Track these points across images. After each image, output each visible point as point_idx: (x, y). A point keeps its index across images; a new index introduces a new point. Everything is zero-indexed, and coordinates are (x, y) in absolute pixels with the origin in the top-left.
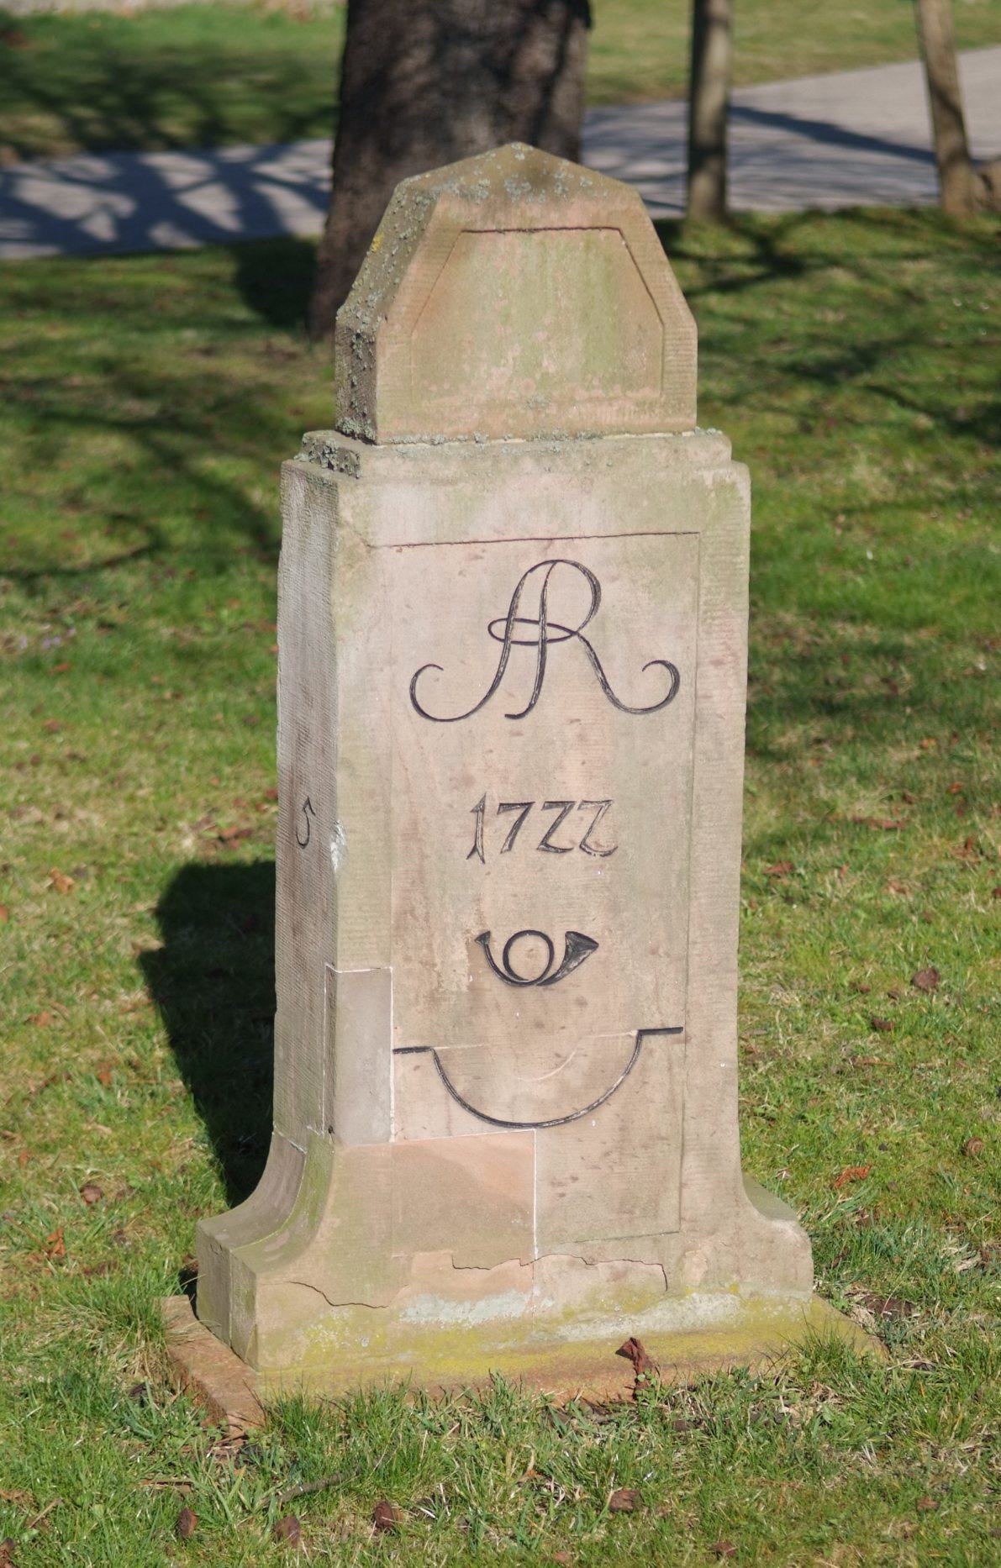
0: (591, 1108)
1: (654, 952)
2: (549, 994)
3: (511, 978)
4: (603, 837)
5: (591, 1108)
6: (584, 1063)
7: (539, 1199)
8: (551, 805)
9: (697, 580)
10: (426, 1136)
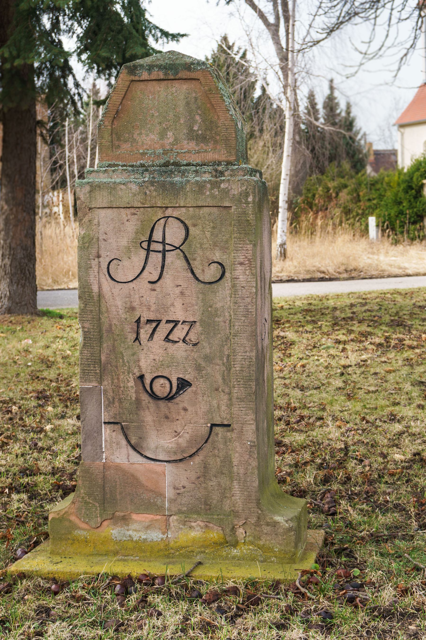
1: (217, 390)
3: (153, 396)
4: (192, 337)
5: (191, 456)
6: (187, 436)
8: (168, 322)
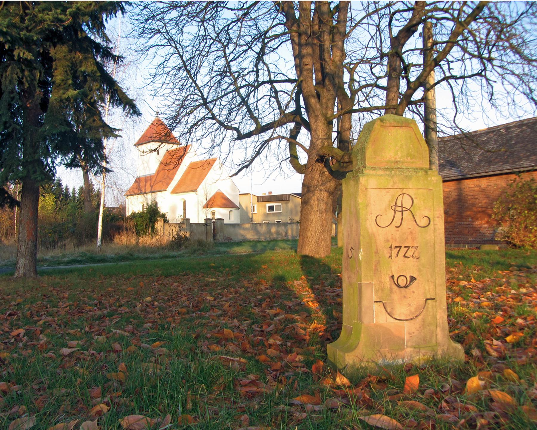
0: (416, 317)
1: (428, 281)
2: (407, 290)
3: (399, 286)
4: (416, 254)
5: (416, 317)
6: (414, 306)
7: (406, 337)
8: (405, 247)
9: (433, 199)
10: (381, 322)
